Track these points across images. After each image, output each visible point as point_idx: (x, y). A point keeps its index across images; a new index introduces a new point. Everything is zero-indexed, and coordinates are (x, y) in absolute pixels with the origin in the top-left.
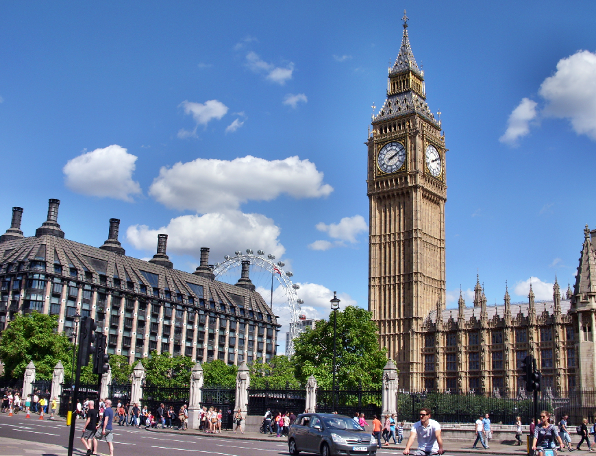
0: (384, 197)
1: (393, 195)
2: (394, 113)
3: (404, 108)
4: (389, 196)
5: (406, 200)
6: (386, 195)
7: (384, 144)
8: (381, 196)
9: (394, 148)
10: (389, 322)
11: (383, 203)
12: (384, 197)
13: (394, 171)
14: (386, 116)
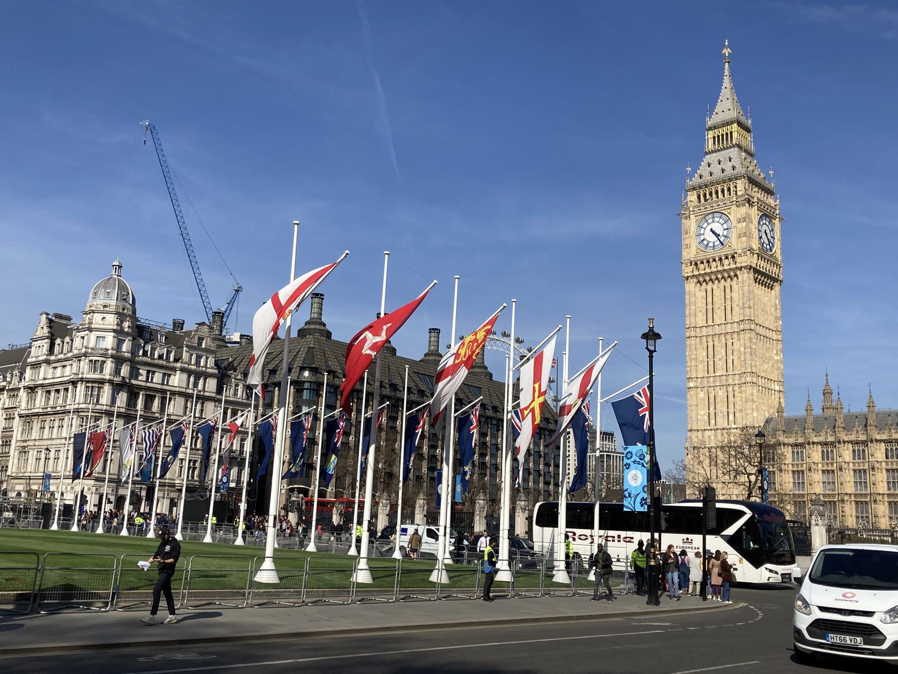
9: (717, 219)
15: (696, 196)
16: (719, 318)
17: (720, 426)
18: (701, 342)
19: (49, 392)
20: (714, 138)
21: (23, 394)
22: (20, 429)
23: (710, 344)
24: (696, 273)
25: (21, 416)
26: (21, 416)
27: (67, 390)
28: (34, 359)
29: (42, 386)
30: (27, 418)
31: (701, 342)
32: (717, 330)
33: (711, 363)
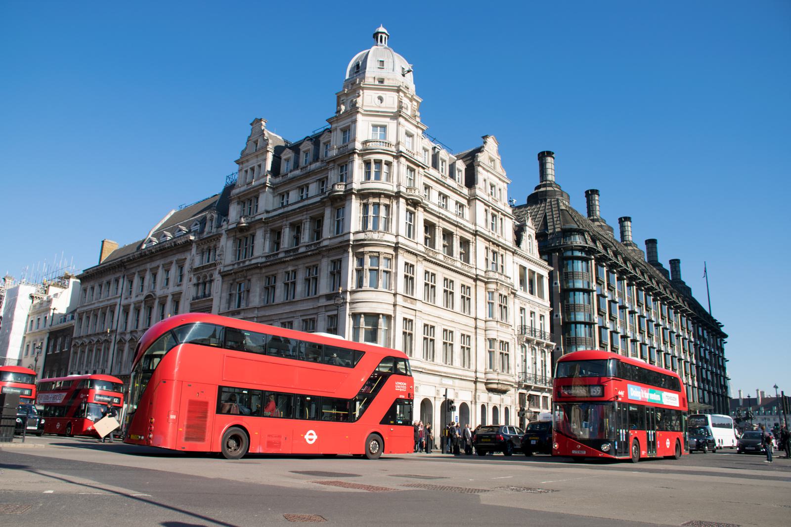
19: (277, 234)
21: (227, 246)
22: (225, 295)
25: (224, 275)
26: (224, 275)
27: (318, 222)
28: (243, 189)
29: (266, 222)
30: (237, 278)
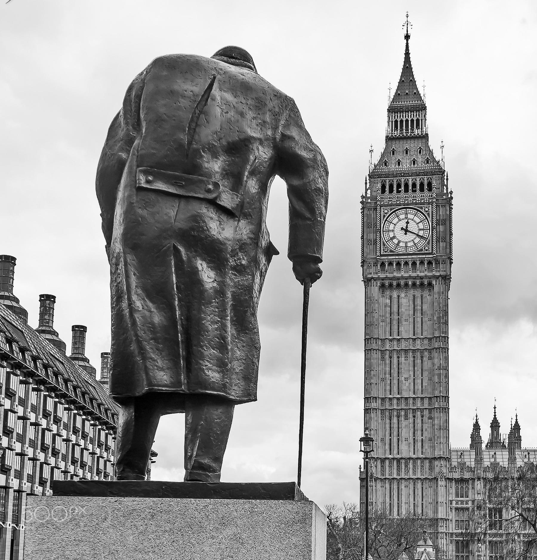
0: (391, 285)
1: (406, 285)
2: (406, 166)
3: (420, 159)
4: (398, 285)
5: (426, 293)
6: (395, 283)
7: (395, 208)
8: (387, 283)
10: (399, 460)
11: (388, 293)
12: (391, 285)
13: (410, 251)
14: (393, 167)
15: (379, 186)
16: (406, 331)
17: (404, 455)
18: (383, 358)
20: (396, 122)
23: (395, 361)
24: (382, 276)
31: (383, 358)
32: (404, 345)
33: (396, 382)
